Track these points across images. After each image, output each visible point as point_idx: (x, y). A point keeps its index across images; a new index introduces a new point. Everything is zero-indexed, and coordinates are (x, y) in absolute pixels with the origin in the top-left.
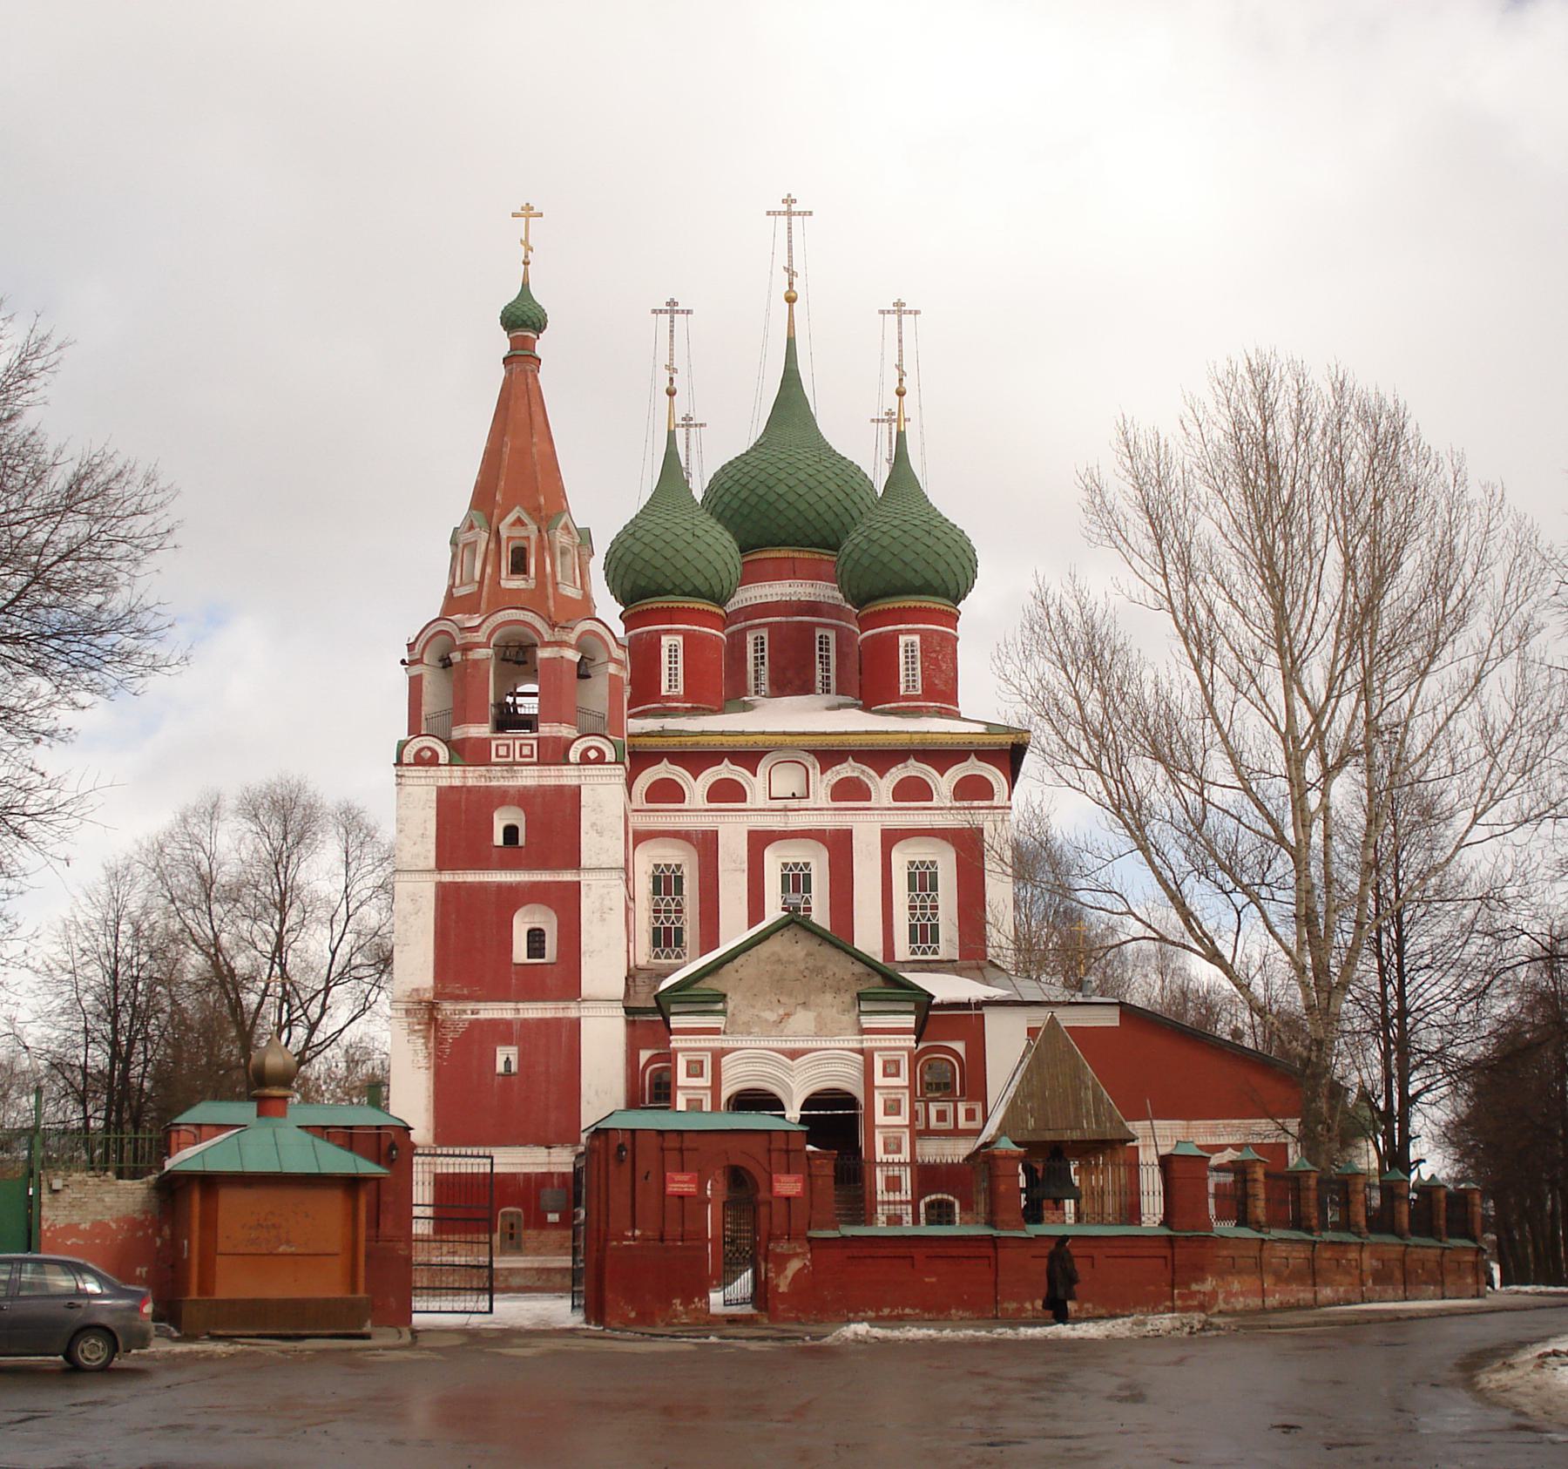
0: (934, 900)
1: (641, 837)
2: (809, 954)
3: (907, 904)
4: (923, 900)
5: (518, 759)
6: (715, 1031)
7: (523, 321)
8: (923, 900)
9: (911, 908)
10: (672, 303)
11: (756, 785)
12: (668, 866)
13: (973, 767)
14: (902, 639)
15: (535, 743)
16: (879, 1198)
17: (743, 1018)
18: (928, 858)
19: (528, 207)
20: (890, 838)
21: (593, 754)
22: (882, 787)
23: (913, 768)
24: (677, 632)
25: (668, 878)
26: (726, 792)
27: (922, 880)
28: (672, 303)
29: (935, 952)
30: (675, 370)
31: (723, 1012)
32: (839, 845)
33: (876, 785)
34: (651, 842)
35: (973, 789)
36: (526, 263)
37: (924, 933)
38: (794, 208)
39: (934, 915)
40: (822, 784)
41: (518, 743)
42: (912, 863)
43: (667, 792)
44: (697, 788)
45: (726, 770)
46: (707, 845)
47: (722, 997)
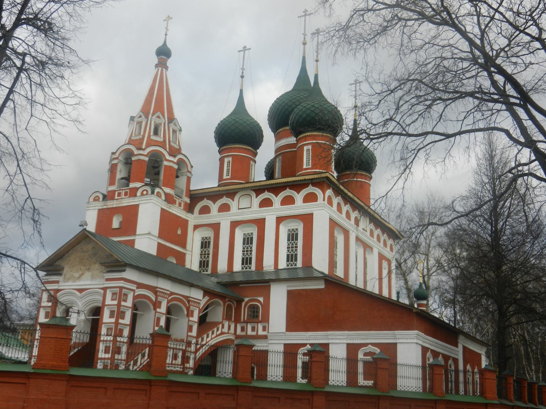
0: (296, 244)
1: (196, 227)
2: (93, 248)
4: (292, 244)
6: (57, 282)
7: (164, 53)
8: (292, 244)
10: (245, 47)
11: (234, 204)
12: (206, 238)
13: (310, 189)
14: (305, 148)
16: (100, 356)
17: (68, 276)
19: (169, 17)
20: (280, 220)
21: (145, 193)
22: (277, 200)
25: (206, 242)
26: (225, 208)
27: (292, 237)
28: (245, 47)
29: (296, 265)
30: (244, 69)
31: (60, 274)
32: (260, 223)
33: (274, 199)
35: (311, 198)
36: (166, 35)
37: (291, 258)
38: (307, 13)
39: (296, 250)
41: (124, 191)
42: (289, 230)
43: (205, 210)
44: (214, 207)
45: (225, 200)
46: (216, 227)
47: (63, 269)
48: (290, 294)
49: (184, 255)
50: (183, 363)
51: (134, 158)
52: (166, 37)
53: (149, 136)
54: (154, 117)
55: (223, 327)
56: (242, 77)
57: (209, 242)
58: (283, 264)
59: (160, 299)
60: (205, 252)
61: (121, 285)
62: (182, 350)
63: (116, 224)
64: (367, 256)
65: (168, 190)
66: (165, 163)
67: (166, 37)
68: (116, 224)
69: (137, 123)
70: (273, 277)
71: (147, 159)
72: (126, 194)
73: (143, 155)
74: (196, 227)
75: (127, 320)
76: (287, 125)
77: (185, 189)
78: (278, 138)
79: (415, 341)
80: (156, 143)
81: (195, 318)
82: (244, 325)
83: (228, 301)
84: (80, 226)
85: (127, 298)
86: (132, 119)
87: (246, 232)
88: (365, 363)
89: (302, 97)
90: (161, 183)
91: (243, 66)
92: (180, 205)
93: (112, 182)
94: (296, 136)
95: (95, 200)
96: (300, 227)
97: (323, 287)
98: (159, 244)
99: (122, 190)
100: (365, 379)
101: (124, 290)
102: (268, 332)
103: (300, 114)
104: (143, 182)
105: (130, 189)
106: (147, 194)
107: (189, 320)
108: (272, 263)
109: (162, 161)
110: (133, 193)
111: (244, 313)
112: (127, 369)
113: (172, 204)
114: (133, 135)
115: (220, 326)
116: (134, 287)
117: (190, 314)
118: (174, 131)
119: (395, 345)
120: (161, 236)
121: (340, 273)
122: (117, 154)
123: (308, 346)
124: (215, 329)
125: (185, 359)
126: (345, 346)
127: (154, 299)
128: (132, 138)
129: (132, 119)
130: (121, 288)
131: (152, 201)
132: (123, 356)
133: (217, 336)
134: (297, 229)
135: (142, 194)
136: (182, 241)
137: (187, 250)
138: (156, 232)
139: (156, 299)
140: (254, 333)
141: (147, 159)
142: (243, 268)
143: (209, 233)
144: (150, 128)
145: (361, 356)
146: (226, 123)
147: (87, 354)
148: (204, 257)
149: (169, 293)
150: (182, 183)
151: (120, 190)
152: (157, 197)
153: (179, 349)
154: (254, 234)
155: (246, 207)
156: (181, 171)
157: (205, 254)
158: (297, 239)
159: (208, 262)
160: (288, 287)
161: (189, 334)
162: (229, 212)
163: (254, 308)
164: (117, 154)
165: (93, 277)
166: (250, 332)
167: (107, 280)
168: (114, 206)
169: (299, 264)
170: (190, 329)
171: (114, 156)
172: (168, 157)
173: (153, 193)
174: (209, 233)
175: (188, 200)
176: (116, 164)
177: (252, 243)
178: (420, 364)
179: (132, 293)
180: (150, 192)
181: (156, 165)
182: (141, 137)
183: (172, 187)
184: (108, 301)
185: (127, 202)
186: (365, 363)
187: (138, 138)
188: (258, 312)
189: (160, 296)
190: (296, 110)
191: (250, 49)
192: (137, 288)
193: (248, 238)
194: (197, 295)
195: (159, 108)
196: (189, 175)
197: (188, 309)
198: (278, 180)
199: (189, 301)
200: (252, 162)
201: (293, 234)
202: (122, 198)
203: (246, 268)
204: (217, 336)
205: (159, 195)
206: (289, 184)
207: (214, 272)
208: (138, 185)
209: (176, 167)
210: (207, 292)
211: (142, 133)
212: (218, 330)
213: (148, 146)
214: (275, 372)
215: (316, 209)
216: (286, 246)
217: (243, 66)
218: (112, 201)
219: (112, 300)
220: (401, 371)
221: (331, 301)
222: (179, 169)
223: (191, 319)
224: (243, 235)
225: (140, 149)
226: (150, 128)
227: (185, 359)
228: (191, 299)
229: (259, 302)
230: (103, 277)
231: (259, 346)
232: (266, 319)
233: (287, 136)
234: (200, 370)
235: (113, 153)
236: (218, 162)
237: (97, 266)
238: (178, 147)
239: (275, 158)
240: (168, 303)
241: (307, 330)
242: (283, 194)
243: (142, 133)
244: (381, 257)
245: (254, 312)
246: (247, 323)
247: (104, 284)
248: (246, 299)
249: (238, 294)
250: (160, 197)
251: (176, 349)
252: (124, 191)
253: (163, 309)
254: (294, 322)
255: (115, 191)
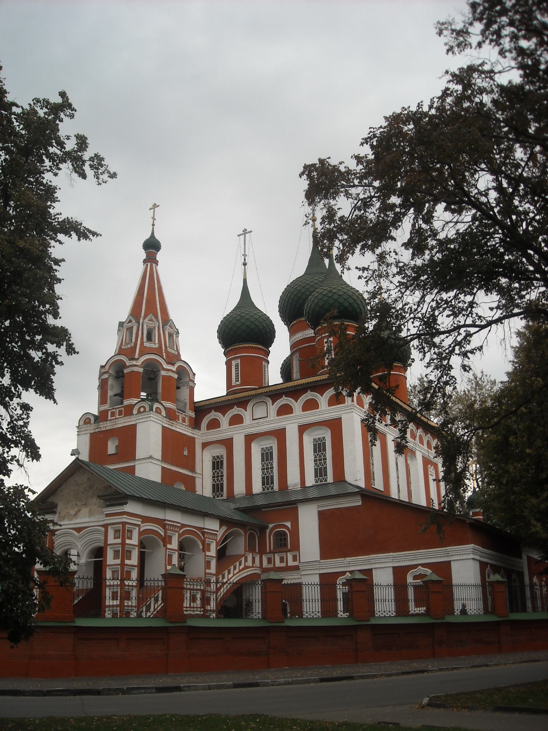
0: (325, 456)
1: (205, 445)
2: (89, 479)
3: (327, 461)
4: (320, 456)
5: (117, 417)
7: (152, 246)
9: (315, 461)
10: (245, 230)
11: (247, 415)
12: (218, 457)
15: (123, 409)
16: (107, 604)
18: (321, 436)
20: (302, 429)
22: (297, 405)
23: (309, 395)
24: (237, 357)
26: (237, 420)
27: (319, 447)
28: (245, 230)
29: (326, 480)
31: (55, 513)
32: (280, 435)
34: (210, 446)
36: (153, 225)
37: (320, 472)
40: (273, 408)
41: (117, 410)
42: (315, 440)
43: (214, 424)
44: (224, 420)
45: (236, 410)
46: (228, 443)
47: (56, 506)
48: (322, 515)
49: (194, 479)
50: (203, 606)
51: (126, 371)
52: (153, 228)
53: (142, 343)
54: (146, 321)
55: (246, 560)
56: (245, 264)
57: (222, 462)
58: (310, 480)
59: (169, 533)
60: (218, 473)
61: (125, 520)
62: (200, 590)
63: (111, 448)
64: (409, 462)
65: (169, 405)
66: (163, 373)
67: (153, 228)
68: (111, 448)
69: (127, 329)
70: (300, 497)
71: (141, 370)
72: (120, 413)
73: (137, 366)
74: (205, 445)
75: (134, 560)
76: (302, 315)
77: (188, 402)
78: (292, 332)
79: (472, 556)
80: (151, 351)
81: (213, 552)
82: (271, 556)
83: (249, 530)
84: (72, 455)
85: (131, 535)
86: (121, 324)
87: (264, 447)
88: (416, 587)
89: (317, 282)
90: (159, 397)
91: (245, 251)
92: (184, 421)
93: (103, 399)
94: (314, 329)
95: (85, 423)
96: (327, 435)
97: (360, 503)
98: (163, 468)
99: (116, 409)
100: (416, 606)
101: (127, 526)
102: (300, 562)
103: (316, 302)
104: (140, 398)
105: (125, 407)
106: (145, 411)
107: (206, 556)
108: (298, 480)
109: (159, 371)
110: (128, 411)
111: (270, 542)
112: (139, 616)
113: (175, 420)
114: (124, 344)
115: (243, 559)
116: (138, 522)
117: (206, 548)
118: (170, 335)
119: (449, 562)
120: (165, 458)
121: (379, 484)
122: (107, 367)
123: (348, 573)
124: (238, 563)
125: (205, 601)
126: (391, 569)
127: (163, 534)
128: (123, 347)
129: (121, 324)
130: (124, 524)
131: (152, 419)
132: (134, 602)
133: (240, 571)
134: (324, 438)
135: (139, 412)
136: (190, 463)
137: (196, 473)
138: (158, 455)
139: (165, 533)
140: (283, 565)
141: (141, 370)
142: (264, 490)
143: (221, 451)
144: (142, 334)
145: (410, 580)
146: (230, 320)
147: (93, 601)
148: (218, 480)
149: (180, 525)
150: (184, 393)
151: (114, 409)
152: (156, 414)
153: (197, 590)
154: (273, 447)
155: (262, 417)
156: (182, 381)
157: (218, 477)
158: (325, 450)
159: (222, 485)
160: (318, 507)
161: (207, 571)
162: (242, 425)
163: (281, 535)
164: (107, 367)
165: (91, 514)
166: (278, 564)
167: (107, 515)
168: (108, 428)
169: (330, 479)
170: (208, 565)
171: (103, 370)
172: (165, 366)
173: (151, 409)
174: (221, 451)
175: (193, 415)
176: (107, 379)
177: (272, 459)
178: (479, 582)
179: (137, 528)
180: (147, 409)
181: (152, 376)
182: (132, 345)
183: (174, 400)
184: (111, 540)
185: (123, 422)
186: (416, 587)
187: (129, 346)
188: (286, 539)
189: (170, 530)
190: (310, 297)
191: (251, 232)
192: (142, 522)
193: (267, 453)
194: (212, 525)
195: (151, 309)
196: (191, 384)
197: (203, 543)
198: (298, 380)
199: (203, 533)
200: (264, 363)
201: (319, 444)
202: (116, 418)
203: (268, 489)
204: (240, 571)
205: (158, 411)
206: (311, 385)
207: (231, 496)
208: (134, 401)
209: (176, 376)
210: (223, 521)
211: (133, 341)
212: (240, 565)
213: (141, 354)
214: (312, 607)
215: (344, 412)
216: (313, 458)
217: (245, 251)
218: (105, 423)
219: (115, 538)
220: (457, 593)
221: (371, 519)
222: (179, 379)
223: (208, 553)
224: (260, 450)
225: (133, 359)
226: (142, 334)
227: (205, 601)
228: (205, 530)
229: (286, 527)
230: (103, 512)
231: (290, 578)
232: (296, 547)
233: (304, 329)
234: (225, 611)
235: (102, 367)
236: (225, 367)
237: (95, 500)
238: (176, 353)
239: (291, 356)
240: (179, 537)
241: (345, 556)
242: (304, 398)
243: (133, 341)
244: (426, 462)
245: (281, 539)
246: (274, 553)
247: (104, 521)
248: (271, 526)
249: (260, 521)
250: (160, 413)
251: (193, 589)
252: (117, 410)
253: (174, 545)
254: (329, 548)
255: (108, 410)
